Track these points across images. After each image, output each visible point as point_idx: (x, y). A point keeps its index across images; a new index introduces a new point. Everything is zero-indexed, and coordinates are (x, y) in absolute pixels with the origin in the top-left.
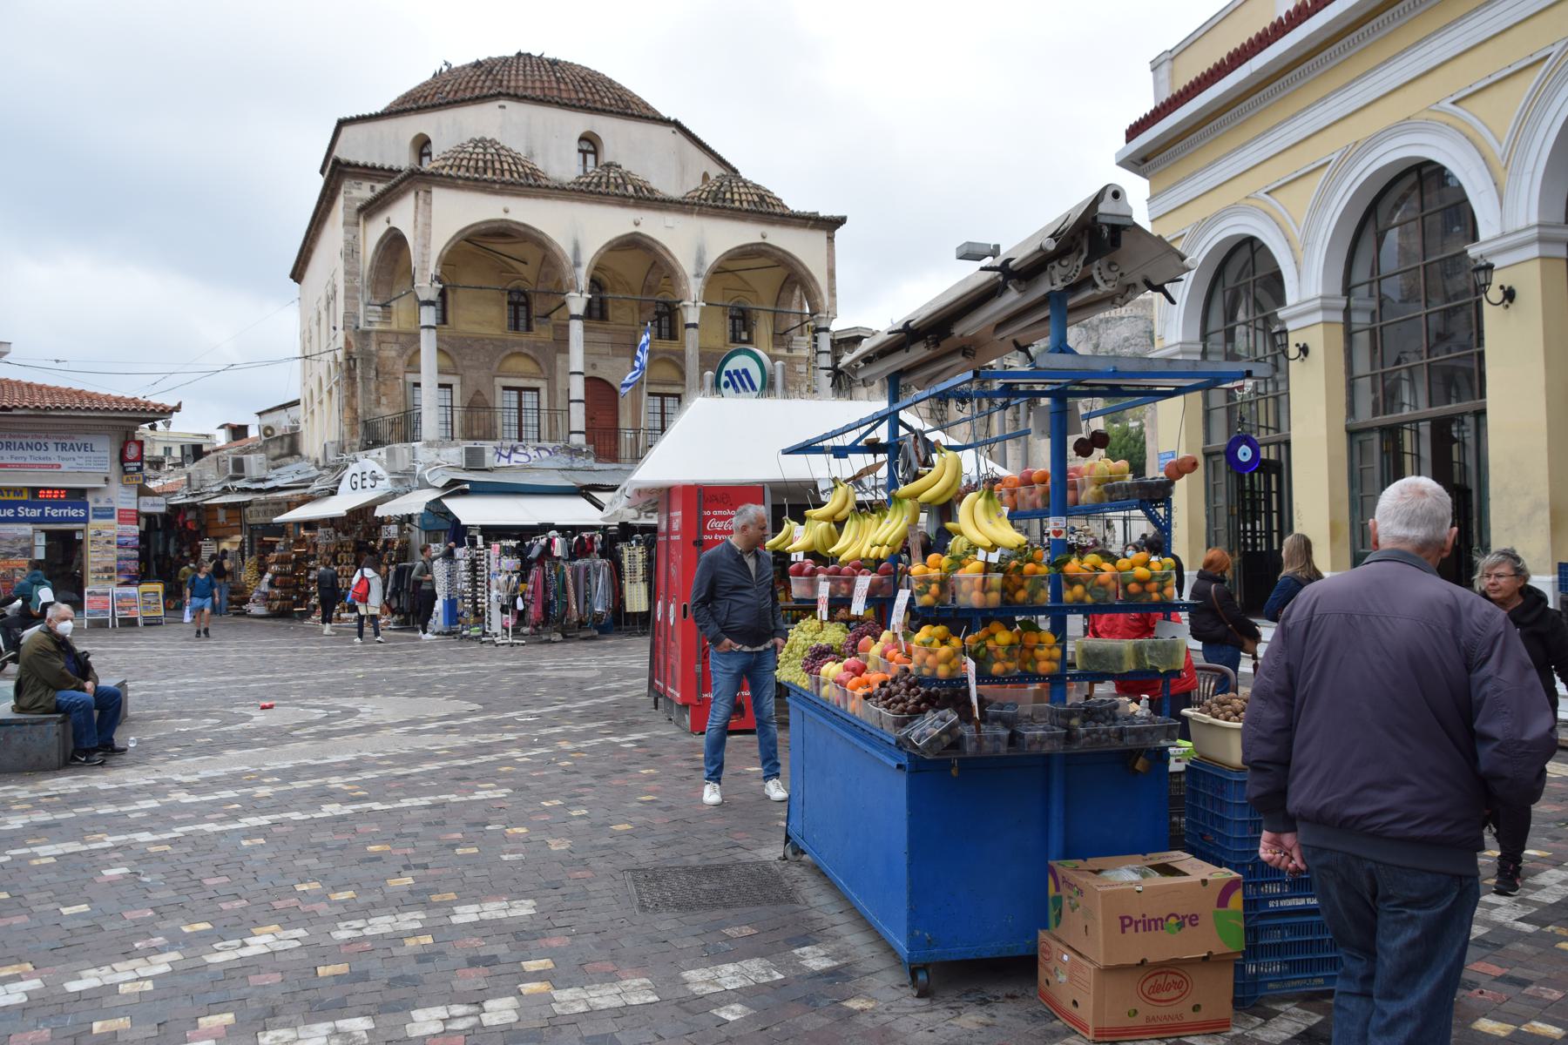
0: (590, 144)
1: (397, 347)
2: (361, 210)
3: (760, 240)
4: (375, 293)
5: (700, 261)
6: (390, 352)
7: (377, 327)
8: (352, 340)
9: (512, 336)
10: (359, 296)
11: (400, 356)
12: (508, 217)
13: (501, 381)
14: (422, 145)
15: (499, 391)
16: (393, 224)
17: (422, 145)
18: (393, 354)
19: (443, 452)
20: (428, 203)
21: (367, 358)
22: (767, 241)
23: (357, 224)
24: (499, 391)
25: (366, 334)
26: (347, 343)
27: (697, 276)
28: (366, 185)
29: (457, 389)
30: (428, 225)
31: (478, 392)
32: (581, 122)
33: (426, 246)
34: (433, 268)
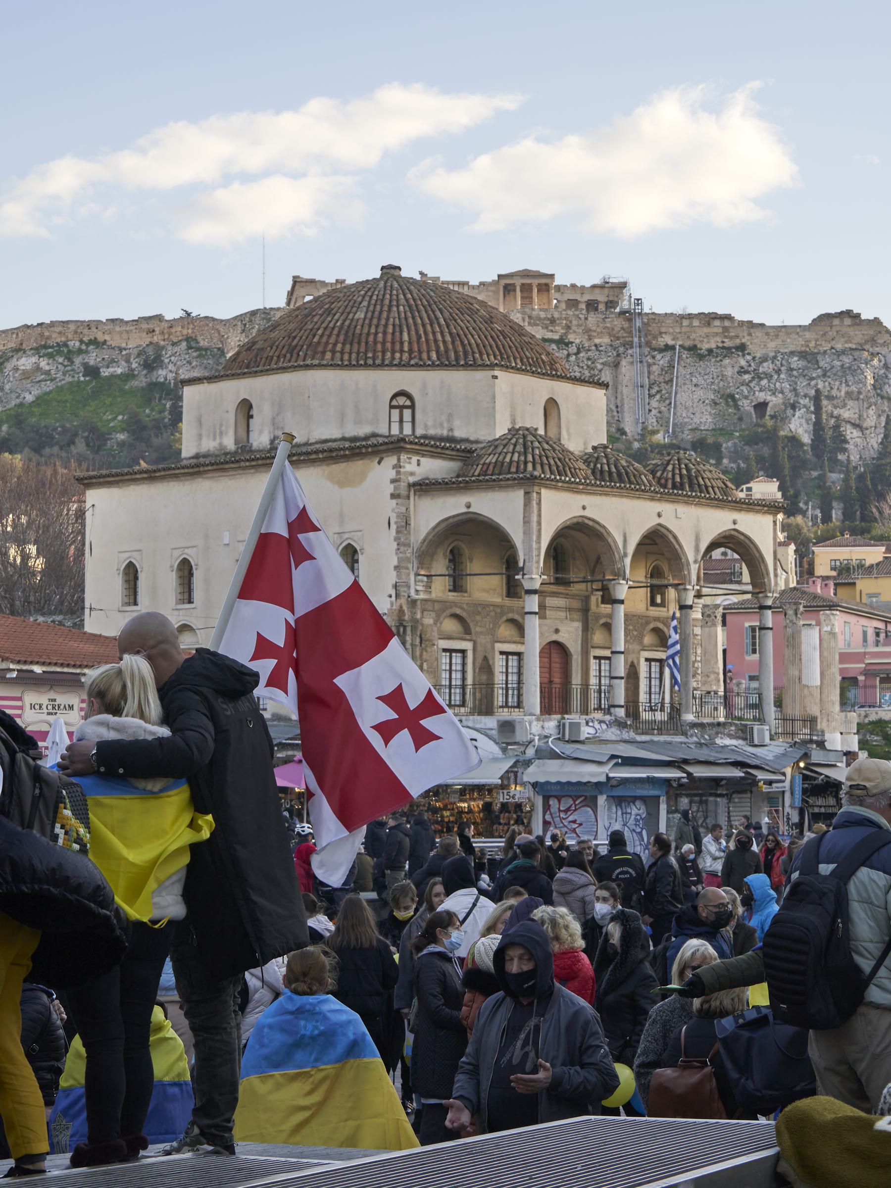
0: (551, 407)
1: (433, 614)
2: (414, 485)
3: (733, 527)
4: (421, 565)
5: (697, 549)
6: (428, 621)
7: (422, 596)
8: (405, 608)
9: (508, 602)
10: (410, 566)
11: (435, 623)
12: (586, 513)
13: (499, 647)
14: (403, 401)
15: (497, 654)
16: (471, 510)
17: (403, 401)
18: (431, 621)
19: (546, 724)
20: (539, 504)
21: (415, 623)
22: (737, 527)
23: (408, 497)
24: (497, 654)
25: (413, 603)
26: (401, 611)
27: (695, 562)
28: (415, 459)
29: (470, 655)
30: (539, 523)
31: (485, 659)
32: (543, 388)
33: (539, 541)
34: (542, 565)
